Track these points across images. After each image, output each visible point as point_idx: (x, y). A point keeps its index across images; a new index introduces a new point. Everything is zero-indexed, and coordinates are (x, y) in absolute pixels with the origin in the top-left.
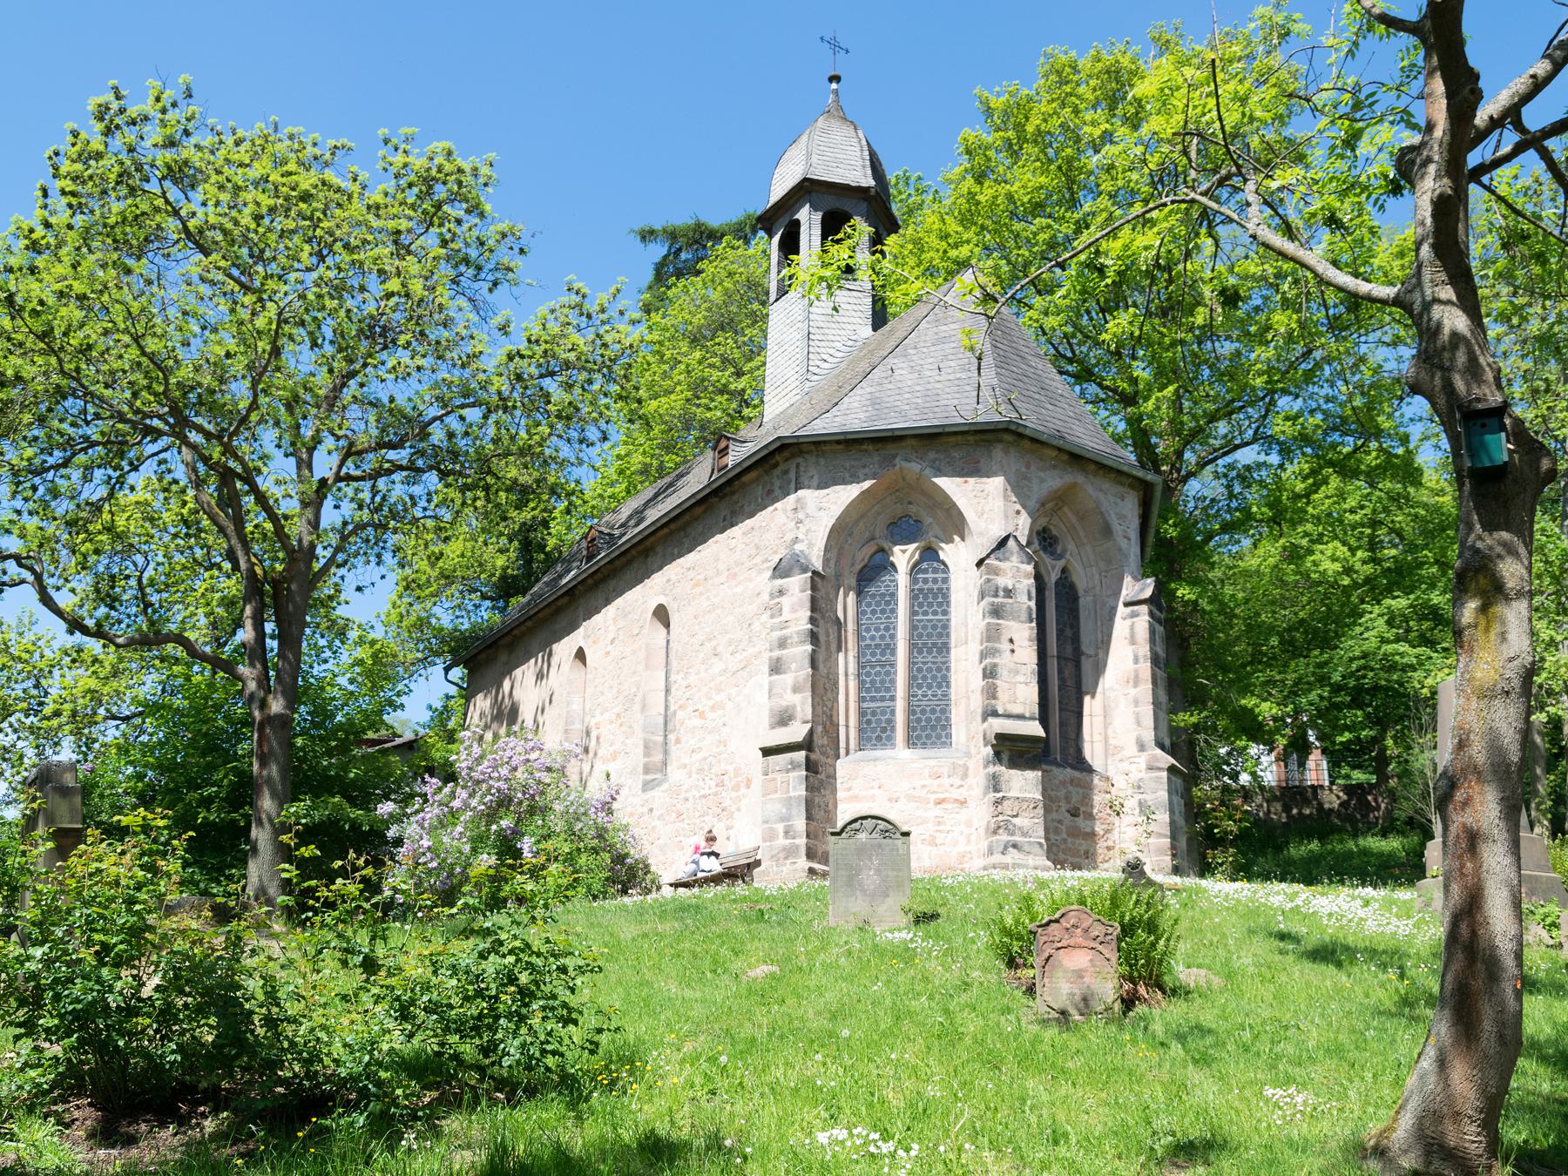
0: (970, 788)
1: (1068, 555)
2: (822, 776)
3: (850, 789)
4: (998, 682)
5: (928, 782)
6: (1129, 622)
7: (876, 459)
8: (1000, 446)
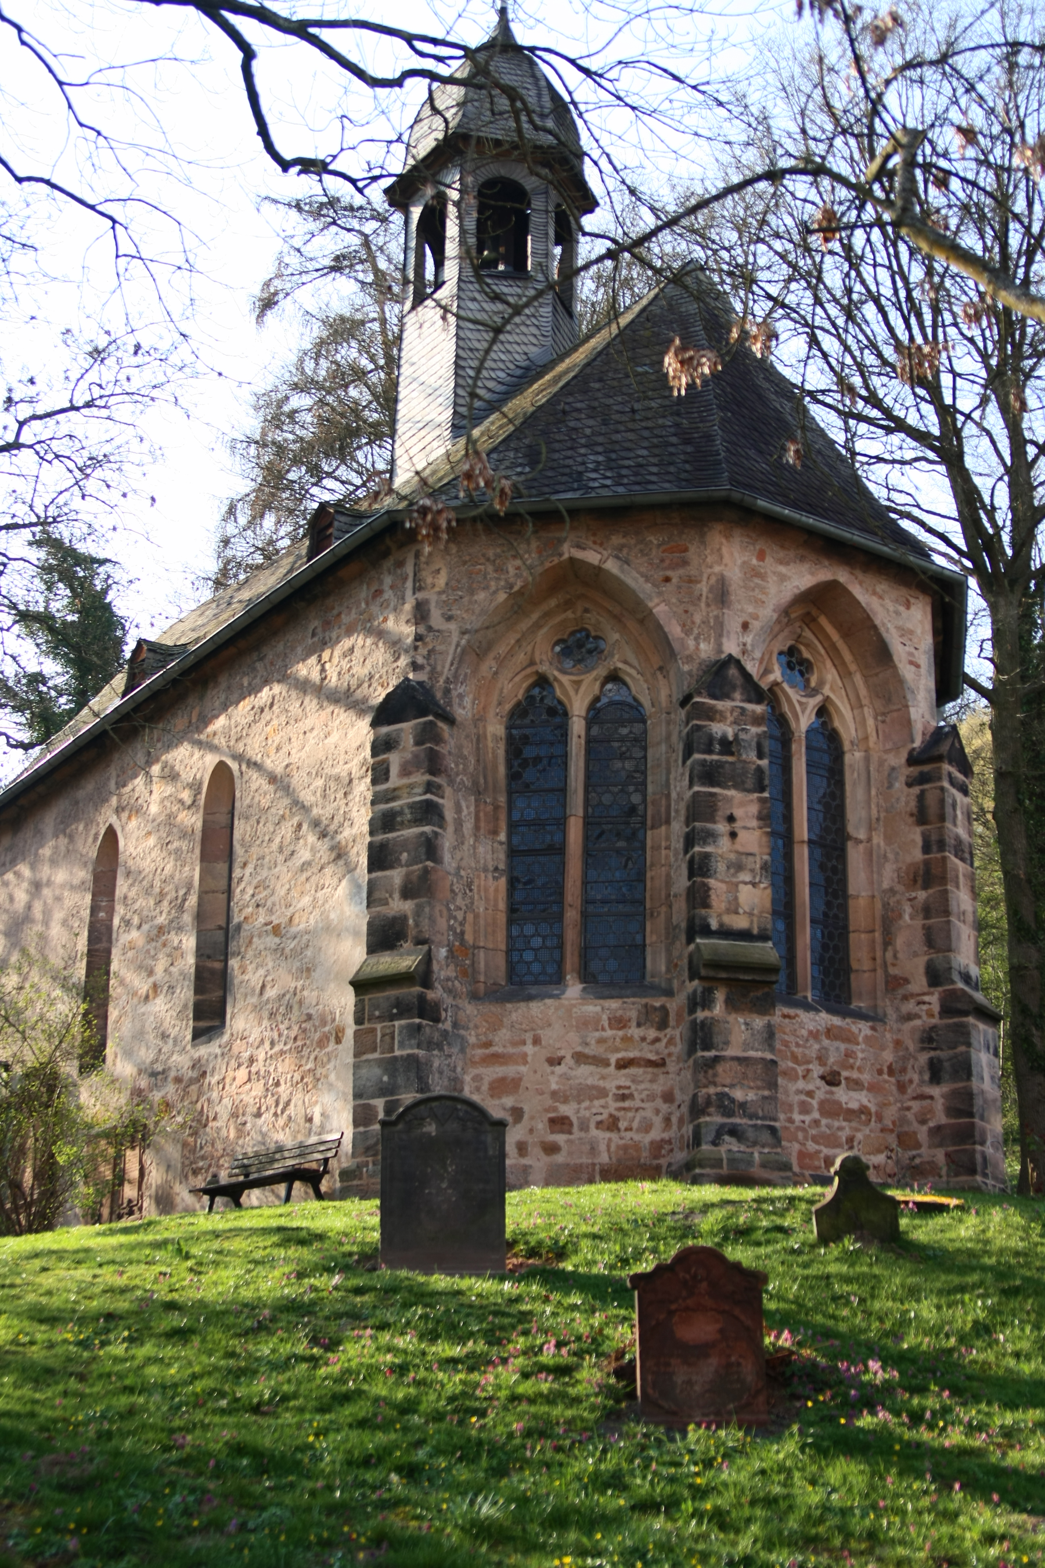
0: (671, 1042)
1: (826, 691)
2: (447, 1026)
3: (488, 1044)
4: (712, 882)
5: (609, 1033)
6: (916, 790)
7: (534, 544)
8: (719, 527)
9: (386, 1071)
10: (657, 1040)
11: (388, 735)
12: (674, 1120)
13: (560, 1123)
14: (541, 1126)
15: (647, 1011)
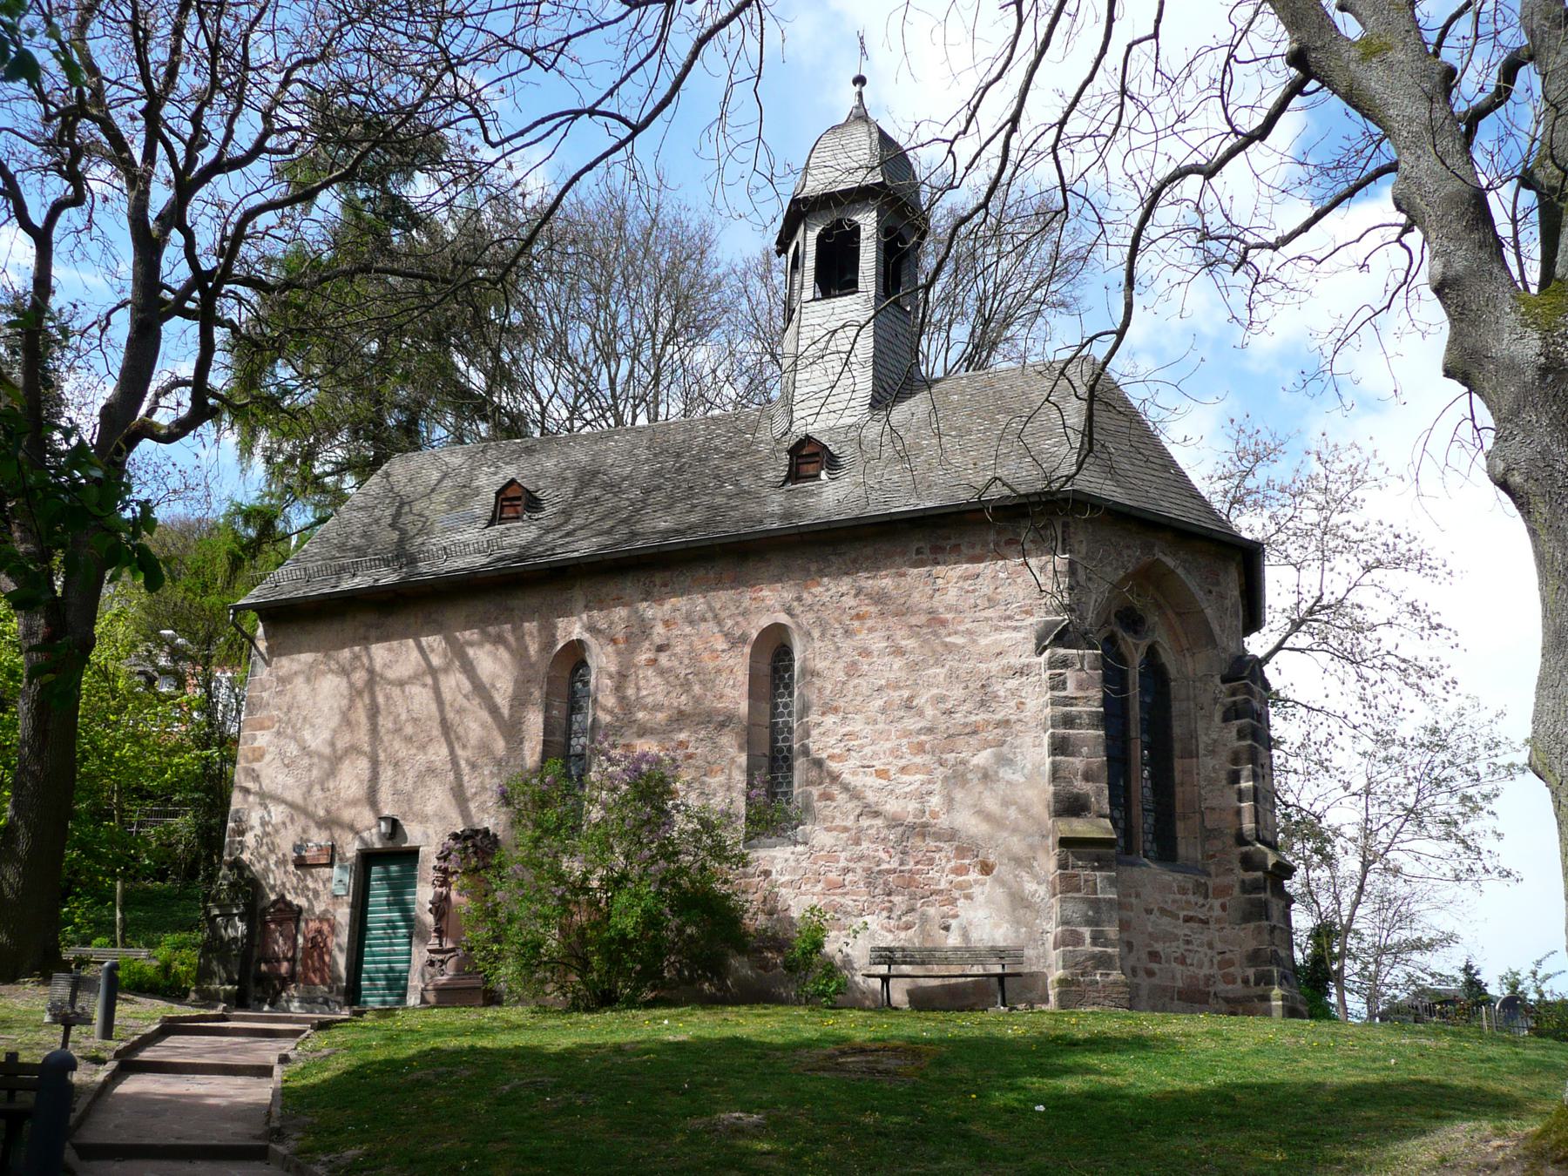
5: (1178, 897)
9: (1090, 908)
10: (1203, 905)
11: (1065, 656)
12: (1215, 961)
13: (1154, 956)
14: (1144, 956)
15: (1198, 885)
